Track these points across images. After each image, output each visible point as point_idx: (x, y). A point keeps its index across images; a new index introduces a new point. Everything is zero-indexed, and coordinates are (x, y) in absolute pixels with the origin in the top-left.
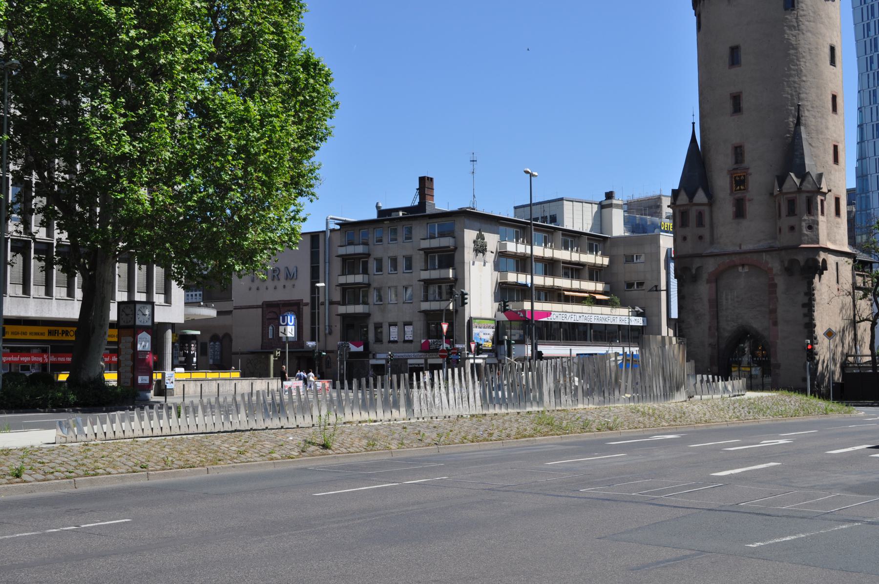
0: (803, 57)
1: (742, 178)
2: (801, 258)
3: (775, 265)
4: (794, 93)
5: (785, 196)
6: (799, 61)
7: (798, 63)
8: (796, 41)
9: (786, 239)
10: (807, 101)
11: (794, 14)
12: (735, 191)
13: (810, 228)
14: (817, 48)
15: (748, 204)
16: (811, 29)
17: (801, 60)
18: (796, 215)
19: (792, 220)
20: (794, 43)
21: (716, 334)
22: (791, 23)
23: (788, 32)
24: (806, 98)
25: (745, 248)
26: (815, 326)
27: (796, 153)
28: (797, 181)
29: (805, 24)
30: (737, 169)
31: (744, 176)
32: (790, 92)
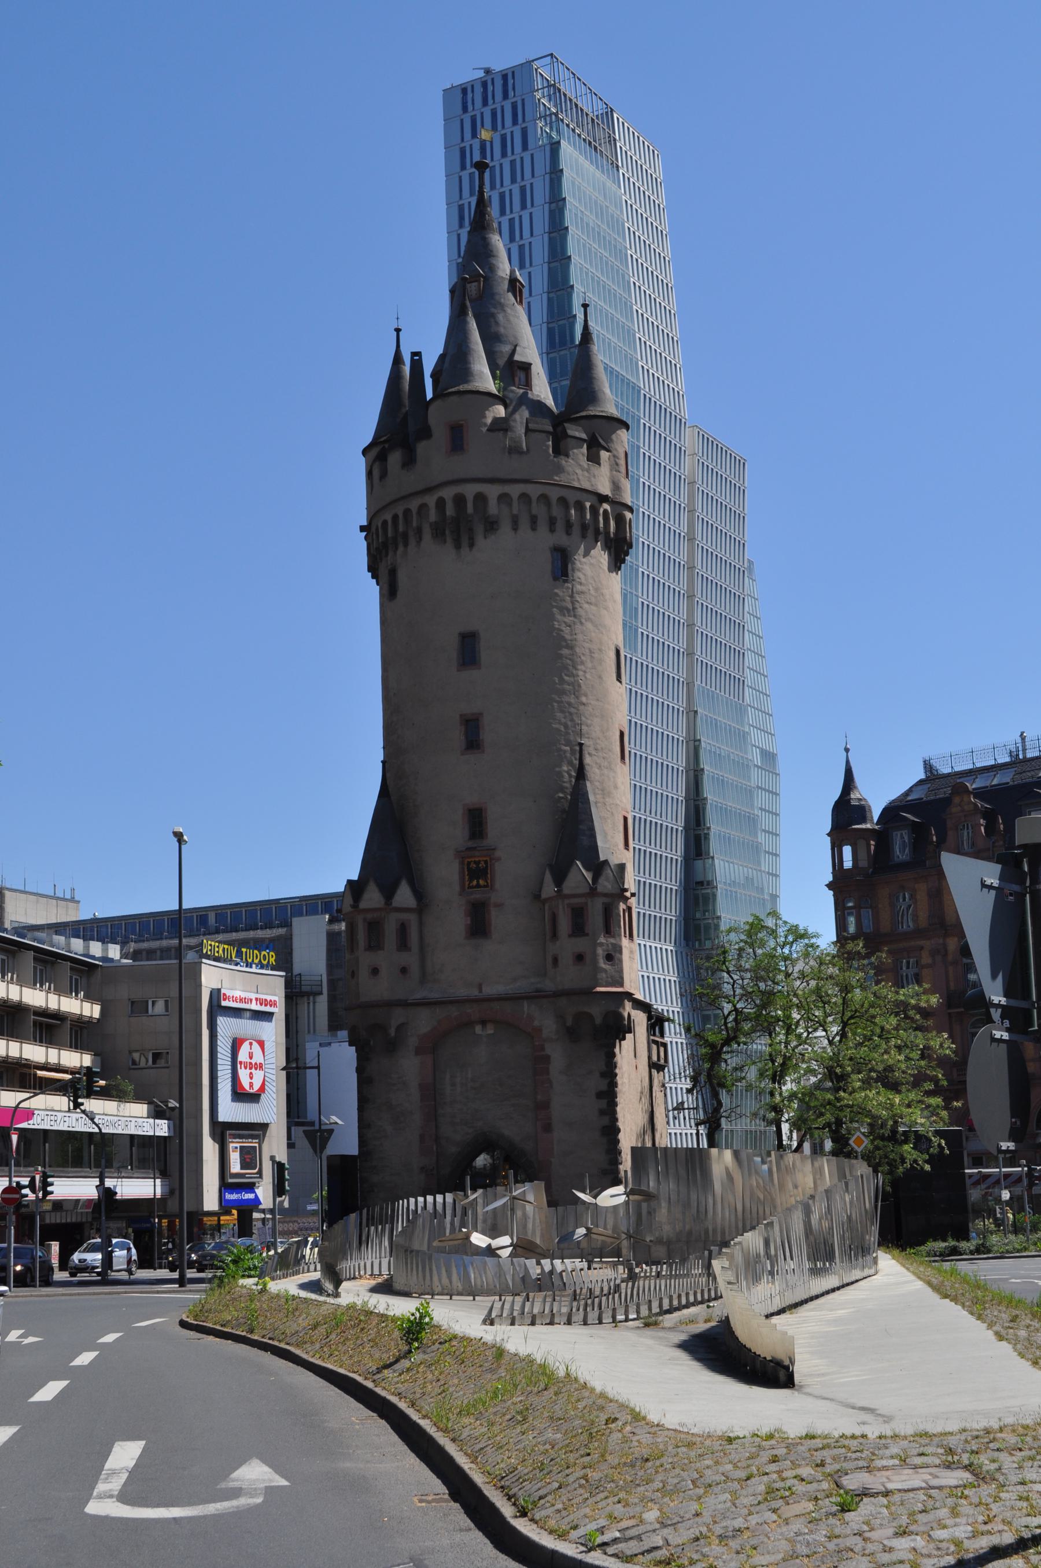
0: (582, 663)
1: (482, 865)
2: (597, 1012)
3: (547, 1024)
4: (569, 723)
5: (567, 901)
6: (576, 669)
7: (574, 672)
8: (571, 635)
9: (569, 976)
10: (588, 738)
11: (568, 588)
12: (470, 887)
13: (609, 958)
14: (600, 650)
15: (494, 912)
16: (592, 617)
17: (579, 667)
18: (587, 935)
19: (580, 944)
20: (568, 637)
21: (435, 1148)
22: (564, 604)
23: (559, 617)
24: (588, 734)
25: (489, 990)
26: (619, 1130)
27: (581, 827)
28: (589, 876)
29: (585, 609)
30: (474, 849)
31: (486, 862)
32: (563, 720)
